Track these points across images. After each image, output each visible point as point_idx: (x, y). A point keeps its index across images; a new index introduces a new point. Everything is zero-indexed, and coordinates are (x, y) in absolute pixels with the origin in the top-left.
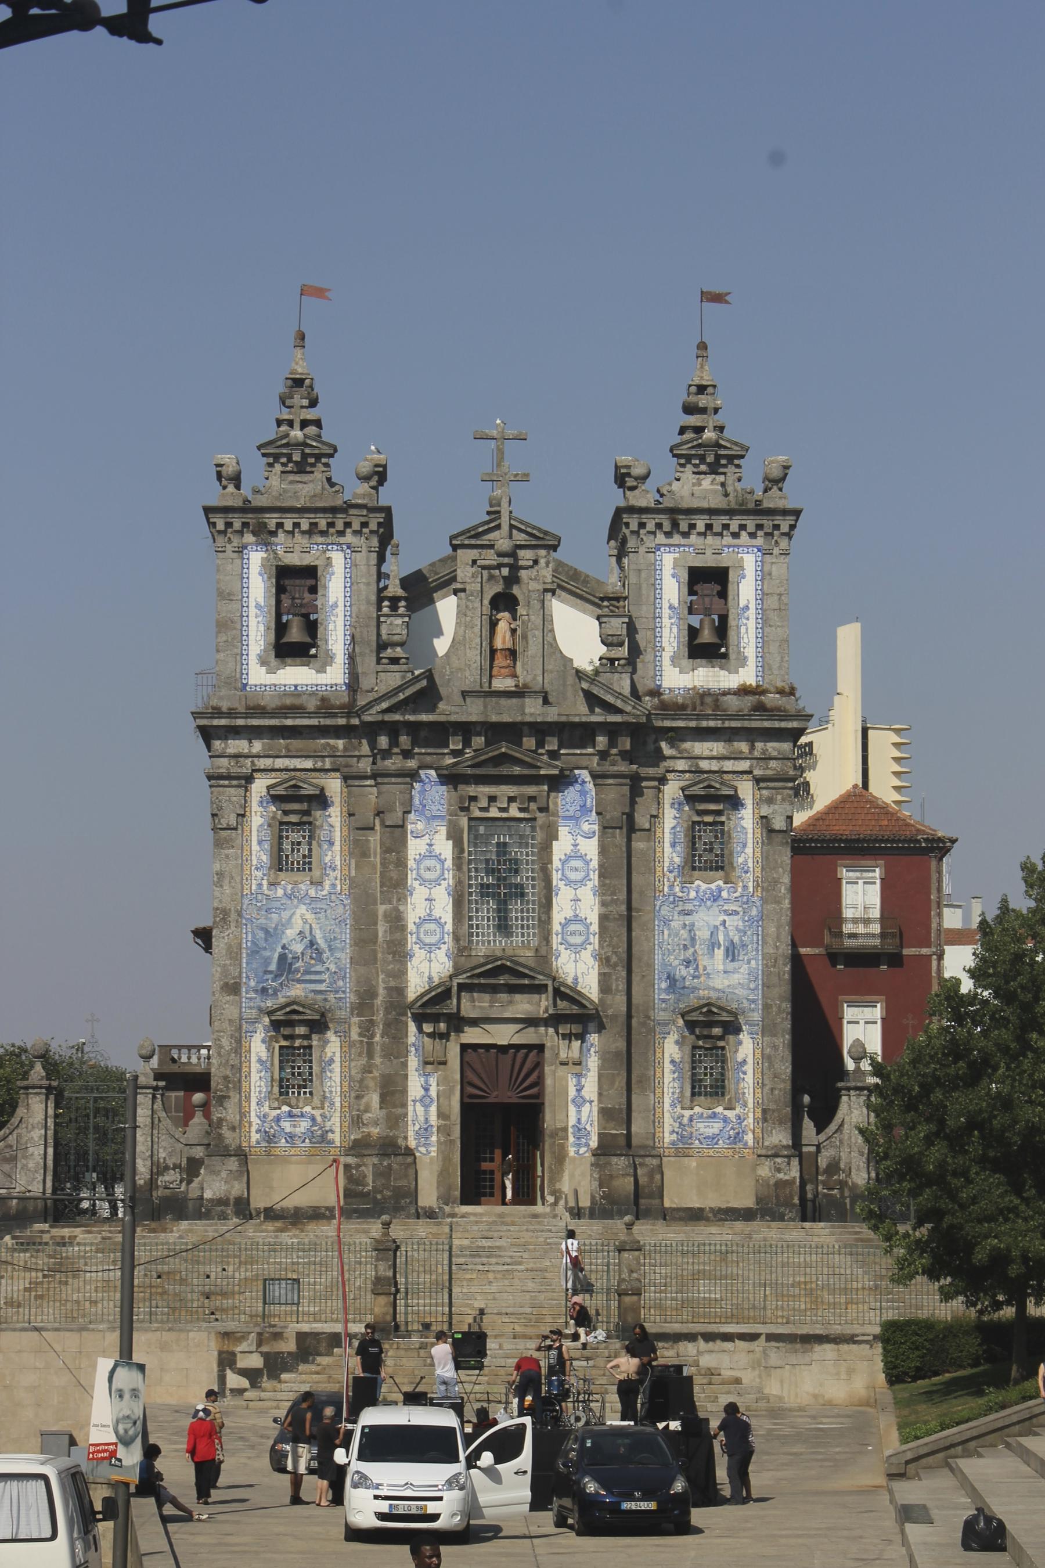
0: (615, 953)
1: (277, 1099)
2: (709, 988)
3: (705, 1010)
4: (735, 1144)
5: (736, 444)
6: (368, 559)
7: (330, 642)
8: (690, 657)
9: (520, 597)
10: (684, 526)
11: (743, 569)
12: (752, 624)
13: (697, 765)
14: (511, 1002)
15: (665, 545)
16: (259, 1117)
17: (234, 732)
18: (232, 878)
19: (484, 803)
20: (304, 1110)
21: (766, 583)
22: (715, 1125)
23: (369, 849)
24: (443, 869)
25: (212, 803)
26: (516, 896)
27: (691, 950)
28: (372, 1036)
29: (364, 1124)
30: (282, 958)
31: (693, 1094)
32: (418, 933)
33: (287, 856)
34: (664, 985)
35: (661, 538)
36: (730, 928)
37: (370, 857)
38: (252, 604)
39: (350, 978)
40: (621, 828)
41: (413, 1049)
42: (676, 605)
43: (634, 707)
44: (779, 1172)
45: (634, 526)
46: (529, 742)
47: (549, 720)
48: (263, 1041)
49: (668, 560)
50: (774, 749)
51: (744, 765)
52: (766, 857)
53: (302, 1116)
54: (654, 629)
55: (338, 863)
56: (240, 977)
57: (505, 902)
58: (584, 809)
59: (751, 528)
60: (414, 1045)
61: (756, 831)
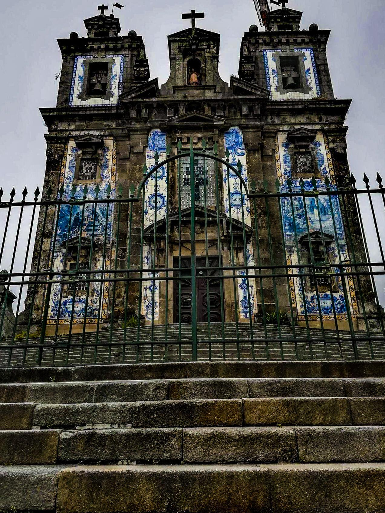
0: (260, 208)
1: (66, 292)
2: (313, 228)
3: (314, 236)
4: (342, 312)
5: (296, 12)
6: (131, 59)
7: (112, 89)
8: (284, 88)
9: (202, 61)
10: (276, 41)
11: (305, 56)
12: (312, 75)
13: (294, 128)
14: (202, 232)
15: (268, 49)
16: (54, 302)
17: (61, 119)
18: (53, 183)
19: (185, 140)
20: (81, 298)
21: (317, 61)
22: (328, 301)
23: (126, 168)
24: (164, 172)
25: (47, 150)
26: (203, 183)
27: (301, 210)
28: (124, 257)
29: (116, 305)
30: (77, 219)
31: (312, 285)
32: (150, 202)
33: (84, 174)
34: (287, 228)
35: (264, 47)
36: (321, 199)
37: (127, 172)
38: (77, 76)
39: (113, 228)
40: (258, 151)
41: (146, 260)
42: (275, 69)
43: (261, 92)
44: (374, 328)
45: (253, 41)
46: (207, 111)
47: (218, 98)
48: (61, 261)
49: (269, 55)
50: (333, 120)
51: (318, 127)
52: (335, 166)
53: (80, 301)
54: (265, 78)
55: (110, 175)
56: (52, 229)
57: (198, 187)
58: (238, 144)
59: (307, 40)
60: (146, 258)
61: (328, 155)
